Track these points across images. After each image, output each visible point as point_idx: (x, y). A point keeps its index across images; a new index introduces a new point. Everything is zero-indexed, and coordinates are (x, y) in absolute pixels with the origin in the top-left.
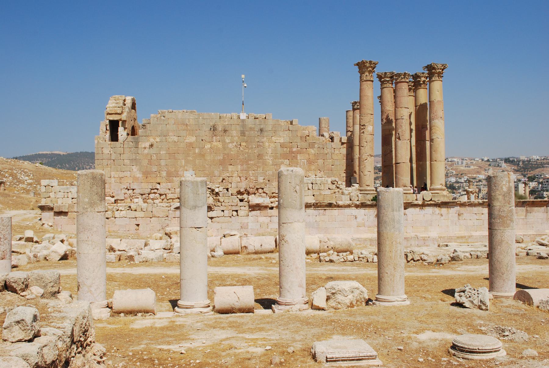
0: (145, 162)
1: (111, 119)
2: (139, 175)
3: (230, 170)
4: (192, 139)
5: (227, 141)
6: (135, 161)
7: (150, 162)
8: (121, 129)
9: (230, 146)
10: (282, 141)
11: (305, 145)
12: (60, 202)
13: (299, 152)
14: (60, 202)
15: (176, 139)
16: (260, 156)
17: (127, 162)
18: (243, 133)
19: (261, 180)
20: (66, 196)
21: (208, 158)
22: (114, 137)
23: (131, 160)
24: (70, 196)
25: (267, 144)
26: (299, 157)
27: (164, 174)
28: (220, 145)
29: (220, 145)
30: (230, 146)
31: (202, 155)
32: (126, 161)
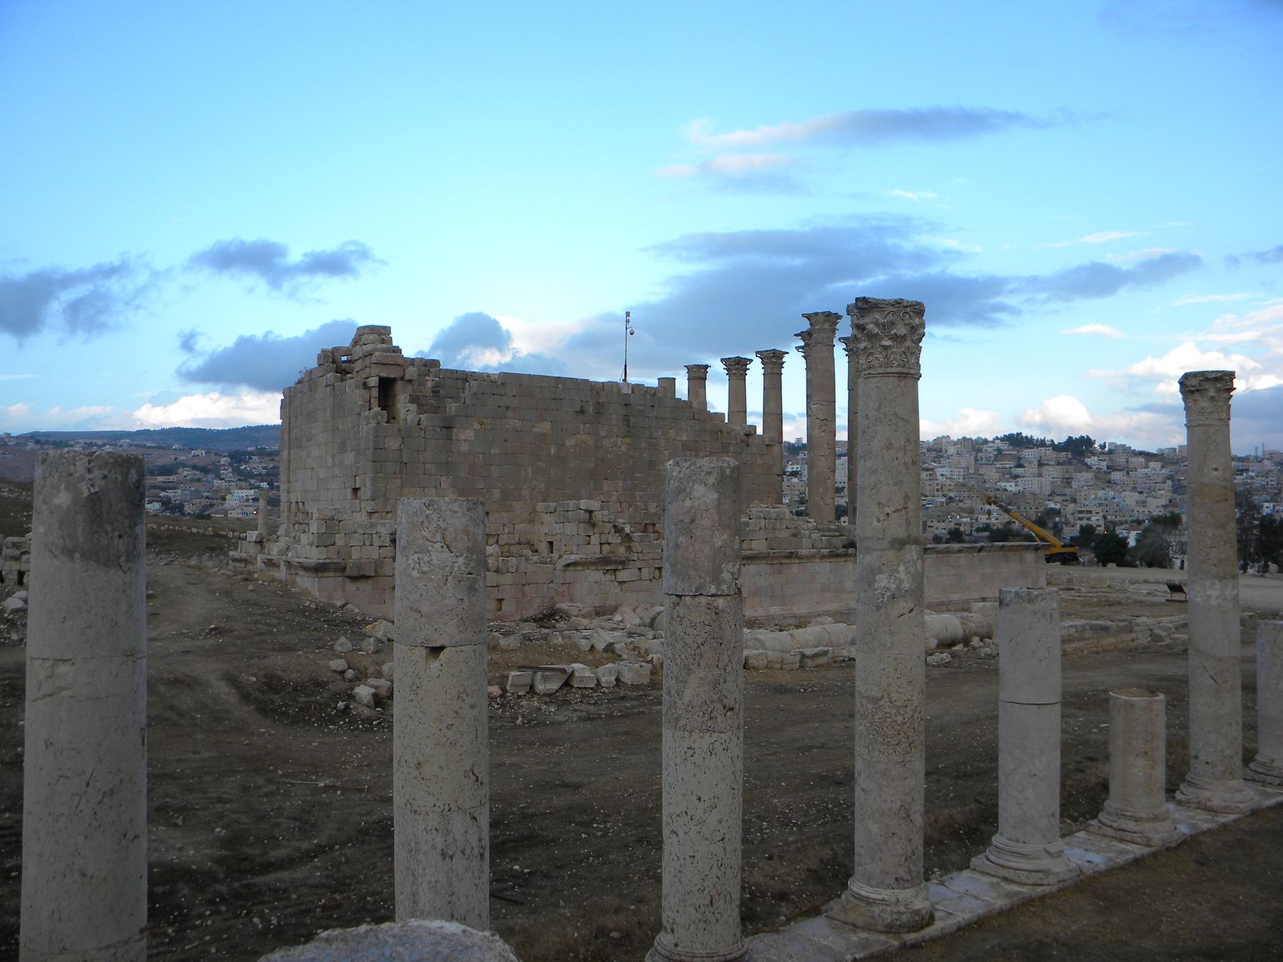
1: (384, 375)
3: (605, 489)
4: (546, 427)
5: (603, 434)
9: (606, 443)
10: (684, 438)
12: (355, 555)
14: (355, 555)
18: (626, 419)
20: (368, 543)
24: (377, 542)
25: (662, 443)
27: (497, 494)
28: (590, 441)
29: (590, 441)
32: (428, 466)
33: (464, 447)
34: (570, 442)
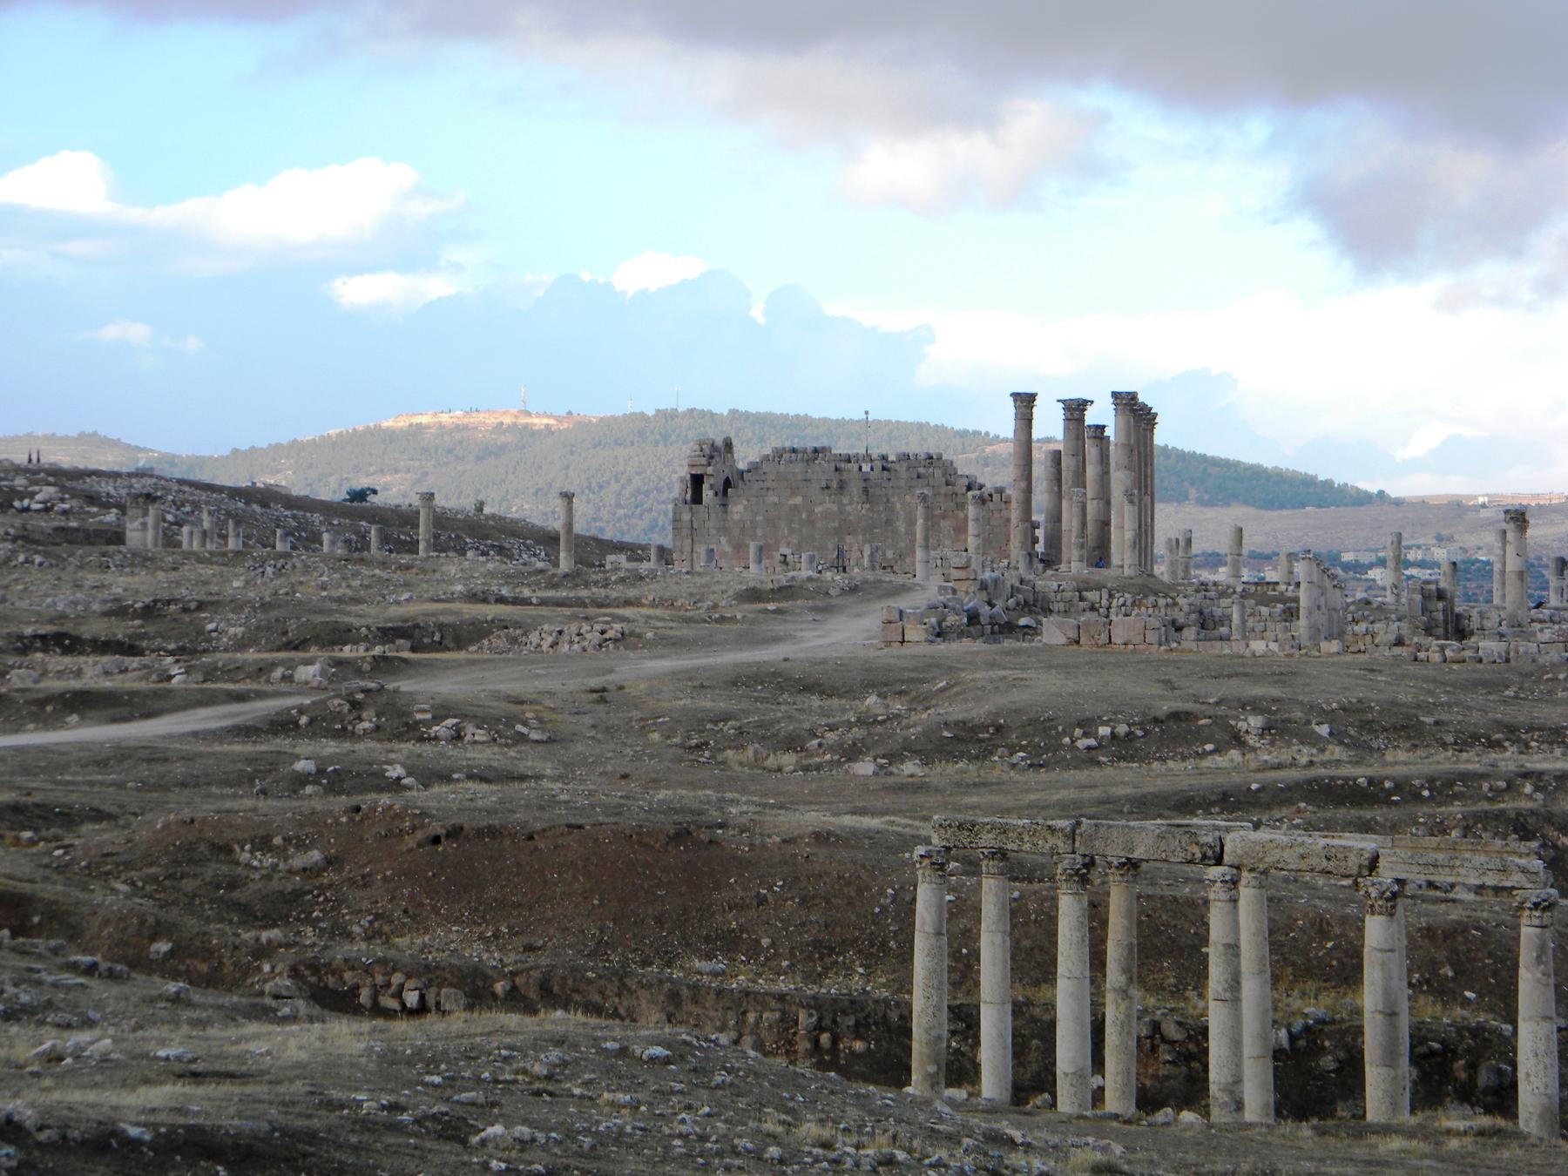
0: (736, 532)
2: (728, 549)
4: (798, 500)
5: (845, 501)
6: (724, 530)
7: (743, 531)
8: (705, 487)
11: (951, 505)
13: (944, 517)
15: (776, 499)
16: (888, 522)
17: (713, 531)
18: (866, 491)
19: (890, 554)
21: (819, 525)
22: (697, 498)
23: (719, 529)
26: (942, 523)
28: (835, 508)
29: (835, 508)
30: (848, 508)
31: (811, 522)
33: (736, 517)
34: (818, 510)
